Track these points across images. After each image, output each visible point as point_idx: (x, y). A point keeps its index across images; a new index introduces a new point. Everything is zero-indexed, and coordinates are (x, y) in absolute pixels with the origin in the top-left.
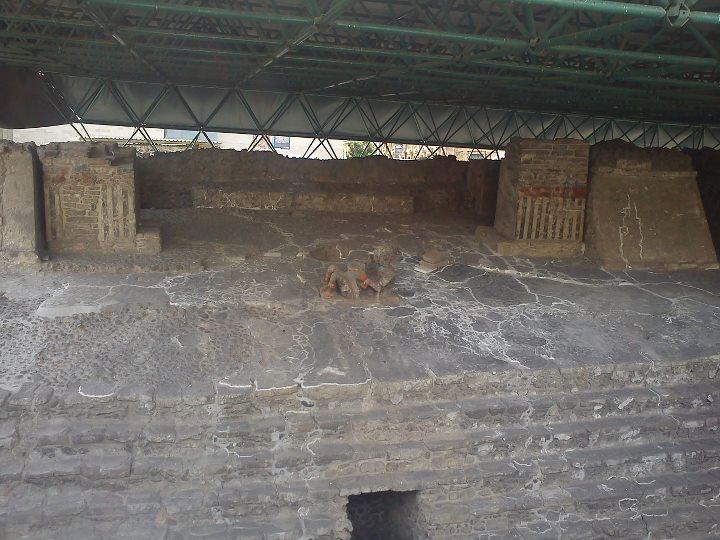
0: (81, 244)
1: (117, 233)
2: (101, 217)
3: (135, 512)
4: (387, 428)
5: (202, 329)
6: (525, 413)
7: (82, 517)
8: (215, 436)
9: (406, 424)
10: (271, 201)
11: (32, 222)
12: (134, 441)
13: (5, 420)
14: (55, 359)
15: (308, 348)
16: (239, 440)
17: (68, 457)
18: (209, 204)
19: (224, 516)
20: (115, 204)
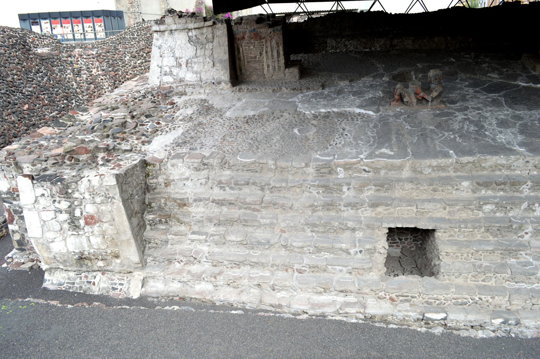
0: (255, 76)
1: (274, 69)
2: (265, 60)
3: (263, 224)
4: (418, 189)
5: (313, 124)
6: (525, 186)
7: (238, 223)
8: (309, 186)
9: (431, 187)
10: (376, 45)
11: (227, 64)
12: (265, 186)
13: (203, 169)
14: (230, 140)
15: (373, 137)
16: (323, 189)
17: (232, 192)
18: (336, 49)
19: (312, 231)
20: (272, 51)
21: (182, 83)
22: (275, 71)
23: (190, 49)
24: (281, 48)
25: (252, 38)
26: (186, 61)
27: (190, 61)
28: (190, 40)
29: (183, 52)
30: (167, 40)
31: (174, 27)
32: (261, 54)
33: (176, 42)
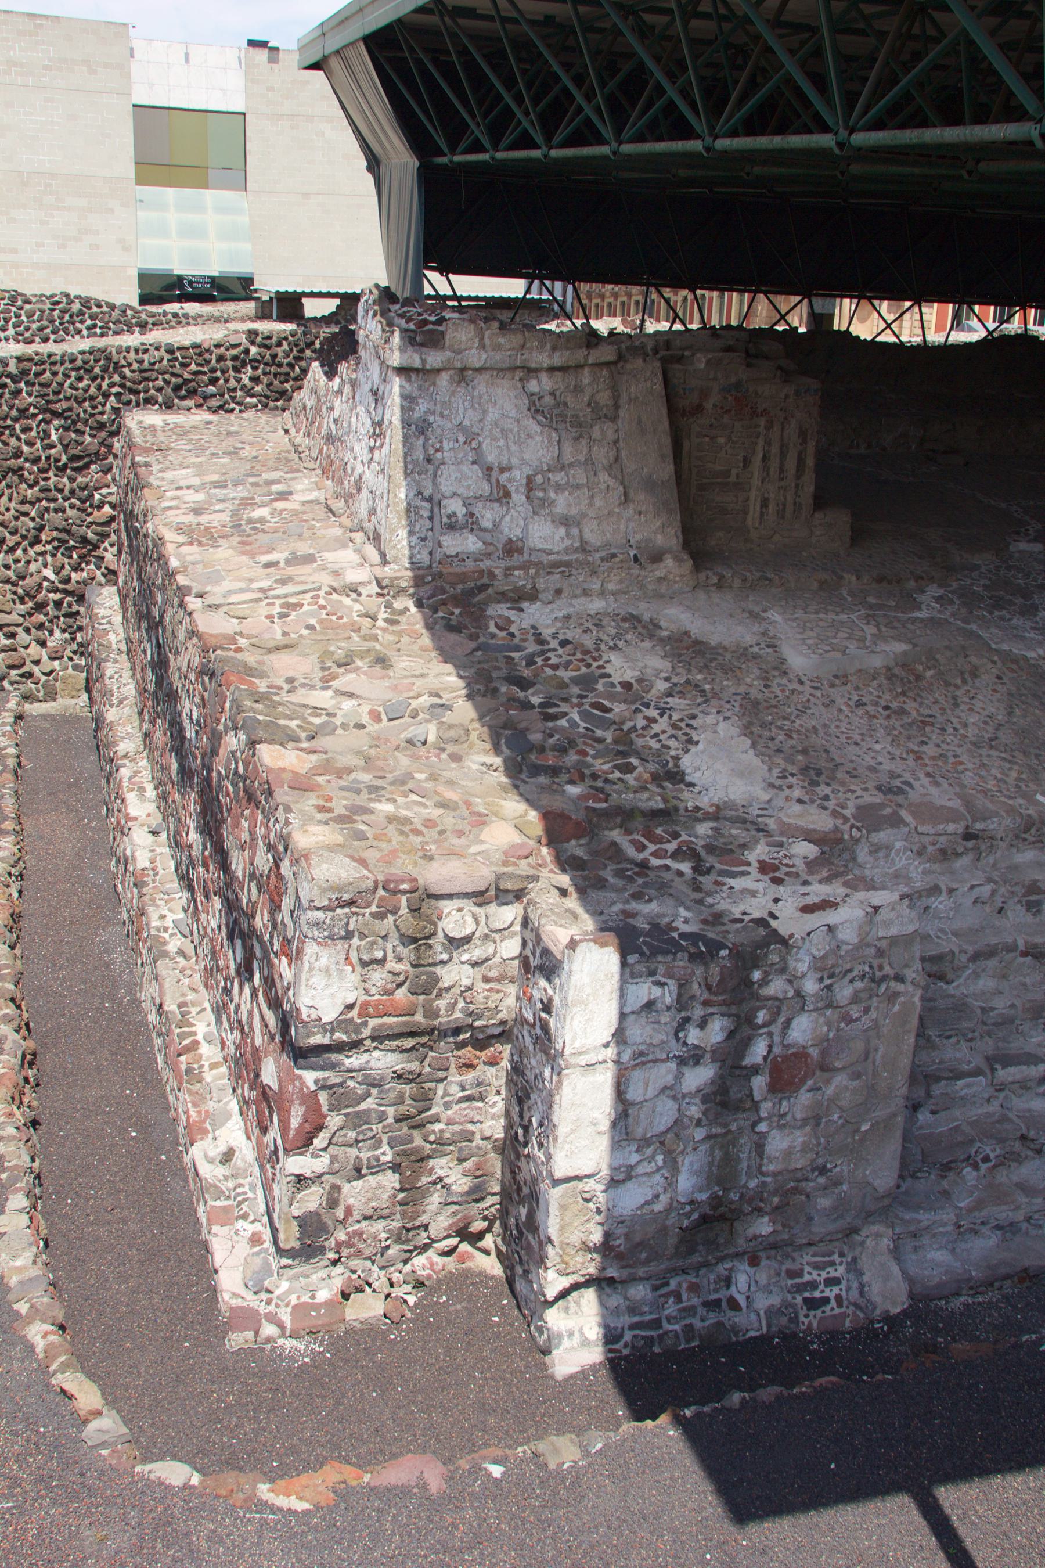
1: (781, 513)
2: (756, 481)
20: (783, 455)
21: (517, 559)
22: (783, 517)
23: (538, 438)
24: (811, 446)
25: (728, 411)
26: (524, 481)
27: (539, 479)
28: (535, 409)
29: (514, 448)
30: (447, 404)
31: (475, 358)
32: (746, 462)
33: (485, 412)
